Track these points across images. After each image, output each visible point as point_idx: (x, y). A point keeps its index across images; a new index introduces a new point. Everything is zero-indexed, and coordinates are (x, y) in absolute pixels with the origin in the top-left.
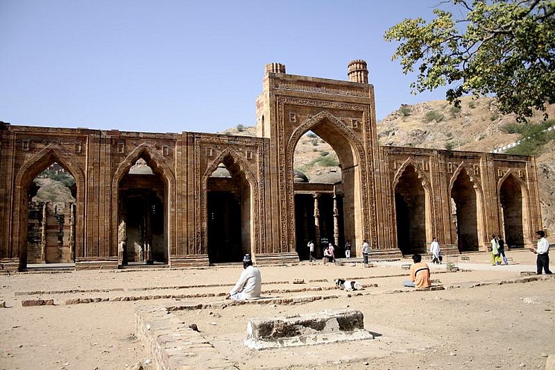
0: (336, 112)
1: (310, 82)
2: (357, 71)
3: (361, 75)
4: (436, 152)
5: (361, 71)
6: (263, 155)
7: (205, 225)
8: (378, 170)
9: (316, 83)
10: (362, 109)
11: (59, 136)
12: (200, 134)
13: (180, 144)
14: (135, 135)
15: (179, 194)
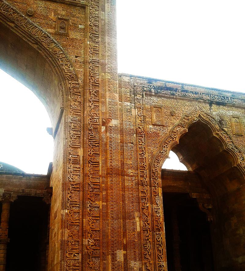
8: (114, 123)
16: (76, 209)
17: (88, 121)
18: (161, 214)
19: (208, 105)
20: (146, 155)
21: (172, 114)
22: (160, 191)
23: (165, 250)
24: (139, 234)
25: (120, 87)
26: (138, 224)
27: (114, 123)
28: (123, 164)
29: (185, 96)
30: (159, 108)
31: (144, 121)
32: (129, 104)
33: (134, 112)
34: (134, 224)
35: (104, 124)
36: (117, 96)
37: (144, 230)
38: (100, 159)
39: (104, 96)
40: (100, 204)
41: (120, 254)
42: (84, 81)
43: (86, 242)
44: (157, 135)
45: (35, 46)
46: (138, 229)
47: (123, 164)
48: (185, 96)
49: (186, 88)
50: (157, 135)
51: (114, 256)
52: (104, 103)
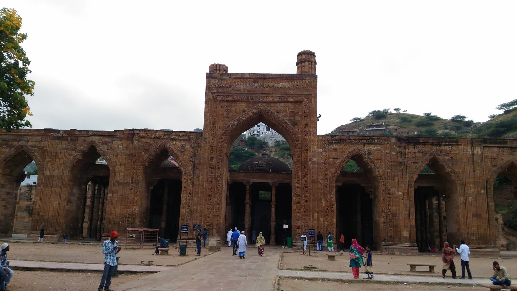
0: (273, 105)
1: (247, 78)
2: (301, 62)
3: (305, 66)
4: (393, 140)
5: (305, 62)
6: (195, 148)
7: (136, 209)
8: (314, 160)
9: (252, 78)
10: (301, 100)
11: (28, 135)
12: (140, 130)
13: (122, 139)
14: (85, 133)
15: (116, 181)
16: (299, 198)
17: (303, 160)
18: (334, 199)
19: (363, 146)
20: (329, 173)
21: (343, 152)
22: (334, 189)
23: (335, 214)
24: (324, 207)
25: (318, 142)
26: (324, 203)
27: (314, 160)
28: (318, 178)
29: (350, 142)
30: (336, 150)
31: (329, 157)
32: (321, 150)
33: (324, 153)
34: (322, 203)
35: (310, 160)
36: (316, 146)
37: (326, 206)
38: (308, 177)
39: (310, 148)
40: (308, 195)
41: (316, 215)
42: (302, 141)
43: (302, 210)
44: (334, 163)
45: (281, 127)
46: (324, 205)
47: (318, 178)
48: (350, 142)
49: (351, 138)
50: (334, 163)
51: (313, 216)
52: (310, 150)
